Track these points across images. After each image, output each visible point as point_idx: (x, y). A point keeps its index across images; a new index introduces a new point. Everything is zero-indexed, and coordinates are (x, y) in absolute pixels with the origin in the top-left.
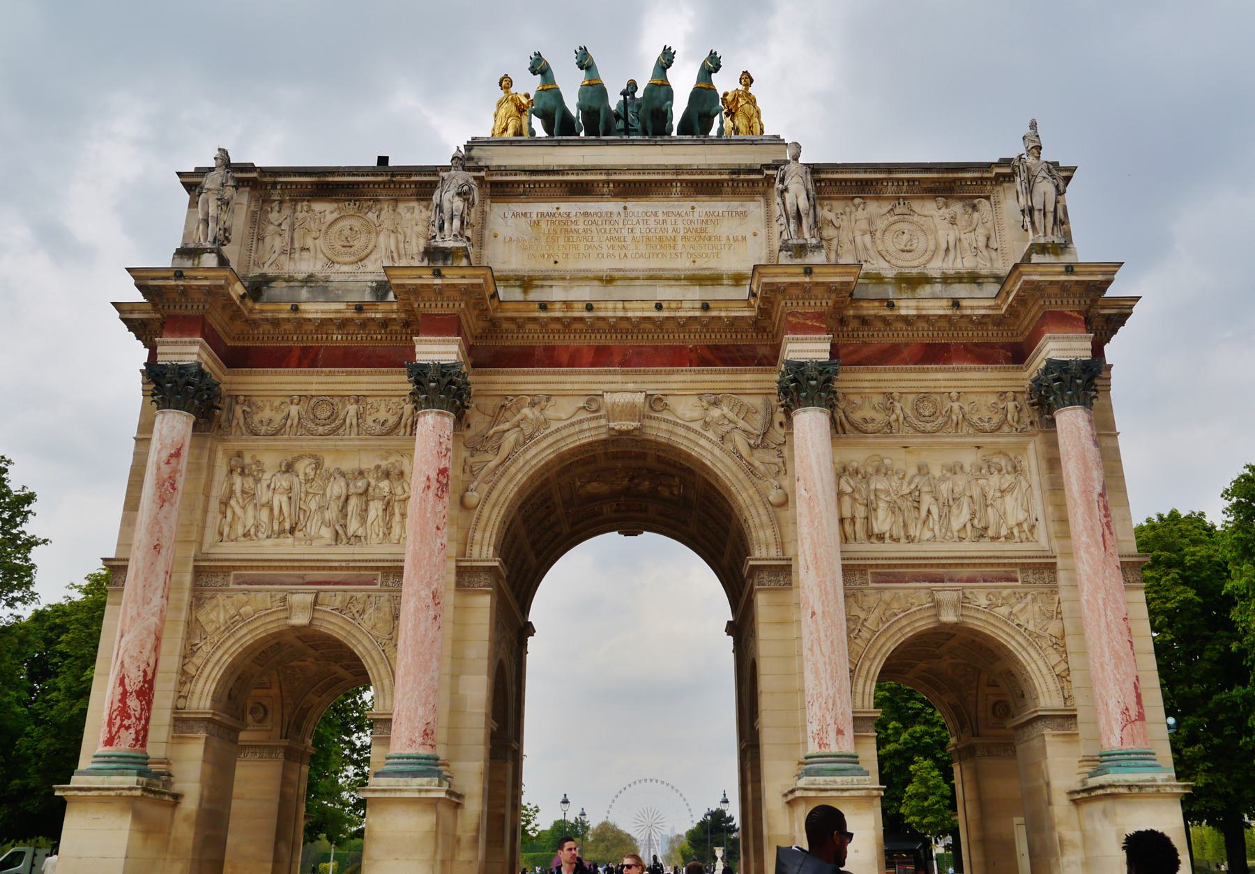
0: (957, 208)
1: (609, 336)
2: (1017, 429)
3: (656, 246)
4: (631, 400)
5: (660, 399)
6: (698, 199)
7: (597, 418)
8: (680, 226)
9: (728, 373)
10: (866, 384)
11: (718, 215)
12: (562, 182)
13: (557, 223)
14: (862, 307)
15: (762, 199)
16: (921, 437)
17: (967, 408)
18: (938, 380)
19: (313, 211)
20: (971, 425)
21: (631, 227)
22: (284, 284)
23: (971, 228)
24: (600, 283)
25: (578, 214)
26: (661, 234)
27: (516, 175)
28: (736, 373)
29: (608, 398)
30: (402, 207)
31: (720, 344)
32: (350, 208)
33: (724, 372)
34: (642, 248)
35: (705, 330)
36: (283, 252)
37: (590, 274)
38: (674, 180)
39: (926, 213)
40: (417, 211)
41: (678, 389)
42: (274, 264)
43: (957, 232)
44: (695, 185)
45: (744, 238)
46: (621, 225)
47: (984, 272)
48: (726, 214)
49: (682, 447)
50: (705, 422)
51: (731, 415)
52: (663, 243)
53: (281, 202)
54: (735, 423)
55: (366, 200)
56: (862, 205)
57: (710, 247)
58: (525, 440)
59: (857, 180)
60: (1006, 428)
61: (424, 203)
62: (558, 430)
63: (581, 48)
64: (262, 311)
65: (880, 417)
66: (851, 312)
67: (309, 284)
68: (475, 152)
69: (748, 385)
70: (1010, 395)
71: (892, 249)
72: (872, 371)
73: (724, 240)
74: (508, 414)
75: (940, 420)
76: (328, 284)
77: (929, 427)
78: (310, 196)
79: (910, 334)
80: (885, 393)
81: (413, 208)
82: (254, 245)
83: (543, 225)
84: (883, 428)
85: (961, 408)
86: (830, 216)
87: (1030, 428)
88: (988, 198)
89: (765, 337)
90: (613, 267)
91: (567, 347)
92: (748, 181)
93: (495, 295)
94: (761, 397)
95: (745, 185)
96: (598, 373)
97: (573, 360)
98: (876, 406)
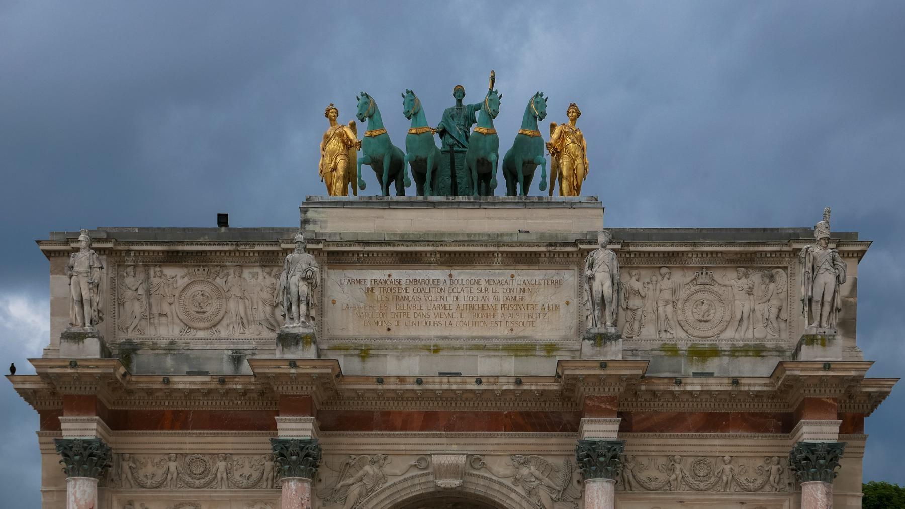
0: (756, 278)
1: (436, 403)
2: (776, 489)
3: (478, 314)
4: (454, 462)
5: (479, 459)
6: (519, 267)
7: (426, 475)
8: (501, 295)
9: (537, 437)
10: (653, 448)
11: (535, 284)
12: (392, 253)
13: (389, 289)
14: (653, 383)
15: (576, 268)
16: (694, 494)
17: (736, 470)
18: (715, 445)
19: (166, 276)
20: (738, 484)
21: (456, 295)
22: (151, 352)
23: (765, 300)
24: (427, 353)
25: (408, 281)
26: (483, 302)
27: (350, 245)
28: (543, 437)
29: (436, 460)
30: (246, 273)
31: (530, 410)
32: (201, 273)
33: (533, 436)
34: (466, 317)
35: (518, 400)
36: (143, 317)
37: (421, 344)
38: (496, 251)
39: (727, 283)
40: (261, 277)
41: (494, 451)
42: (136, 329)
43: (752, 303)
44: (514, 256)
45: (558, 307)
46: (447, 292)
47: (769, 344)
48: (542, 282)
49: (496, 500)
50: (516, 479)
51: (537, 473)
52: (485, 311)
53: (135, 267)
54: (540, 480)
55: (214, 266)
56: (667, 276)
57: (527, 316)
58: (367, 493)
59: (664, 253)
60: (767, 488)
61: (268, 270)
62: (394, 485)
63: (408, 92)
64: (137, 383)
65: (662, 477)
66: (643, 388)
67: (172, 352)
68: (311, 214)
69: (553, 448)
70: (775, 459)
71: (691, 319)
72: (659, 437)
73: (539, 308)
74: (352, 471)
75: (713, 480)
76: (188, 352)
77: (702, 486)
78: (161, 262)
79: (695, 404)
80: (668, 456)
81: (258, 273)
82: (116, 309)
83: (377, 293)
84: (664, 486)
85: (731, 470)
86: (637, 286)
87: (788, 488)
88: (785, 268)
89: (569, 406)
90: (439, 334)
91: (400, 412)
92: (563, 253)
93: (339, 375)
94: (563, 458)
95: (561, 256)
96: (427, 436)
97: (406, 424)
98: (660, 467)
